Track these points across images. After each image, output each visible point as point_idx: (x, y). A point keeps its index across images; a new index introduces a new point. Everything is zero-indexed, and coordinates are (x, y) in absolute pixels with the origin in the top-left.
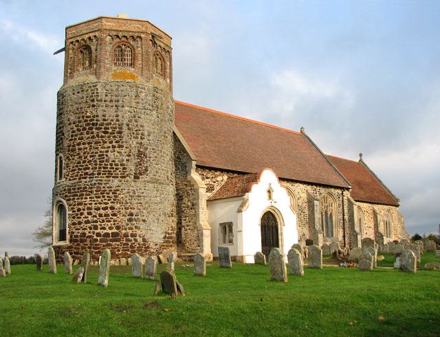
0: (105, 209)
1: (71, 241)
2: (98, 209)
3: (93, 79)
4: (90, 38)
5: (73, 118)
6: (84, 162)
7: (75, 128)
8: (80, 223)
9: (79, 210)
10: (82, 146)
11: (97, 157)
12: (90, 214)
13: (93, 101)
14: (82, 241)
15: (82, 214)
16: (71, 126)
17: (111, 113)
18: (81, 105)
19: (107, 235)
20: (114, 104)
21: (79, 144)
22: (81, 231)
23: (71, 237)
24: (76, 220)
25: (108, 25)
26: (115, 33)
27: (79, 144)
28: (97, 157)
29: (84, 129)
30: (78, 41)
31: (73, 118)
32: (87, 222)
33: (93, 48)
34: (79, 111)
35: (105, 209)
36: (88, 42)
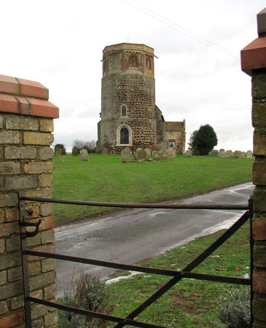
0: (148, 132)
1: (133, 144)
2: (145, 131)
3: (140, 73)
4: (137, 53)
5: (132, 89)
6: (139, 110)
7: (133, 94)
8: (138, 137)
9: (138, 131)
10: (137, 103)
11: (144, 109)
12: (142, 133)
13: (142, 84)
14: (139, 145)
15: (139, 133)
16: (132, 93)
17: (148, 90)
18: (137, 85)
19: (148, 142)
20: (149, 86)
21: (136, 102)
22: (139, 140)
23: (134, 142)
24: (136, 136)
25: (145, 49)
26: (146, 53)
27: (136, 102)
28: (144, 109)
29: (138, 96)
30: (130, 52)
31: (132, 89)
32: (142, 137)
33: (139, 58)
34: (135, 87)
35: (148, 132)
36: (136, 54)
